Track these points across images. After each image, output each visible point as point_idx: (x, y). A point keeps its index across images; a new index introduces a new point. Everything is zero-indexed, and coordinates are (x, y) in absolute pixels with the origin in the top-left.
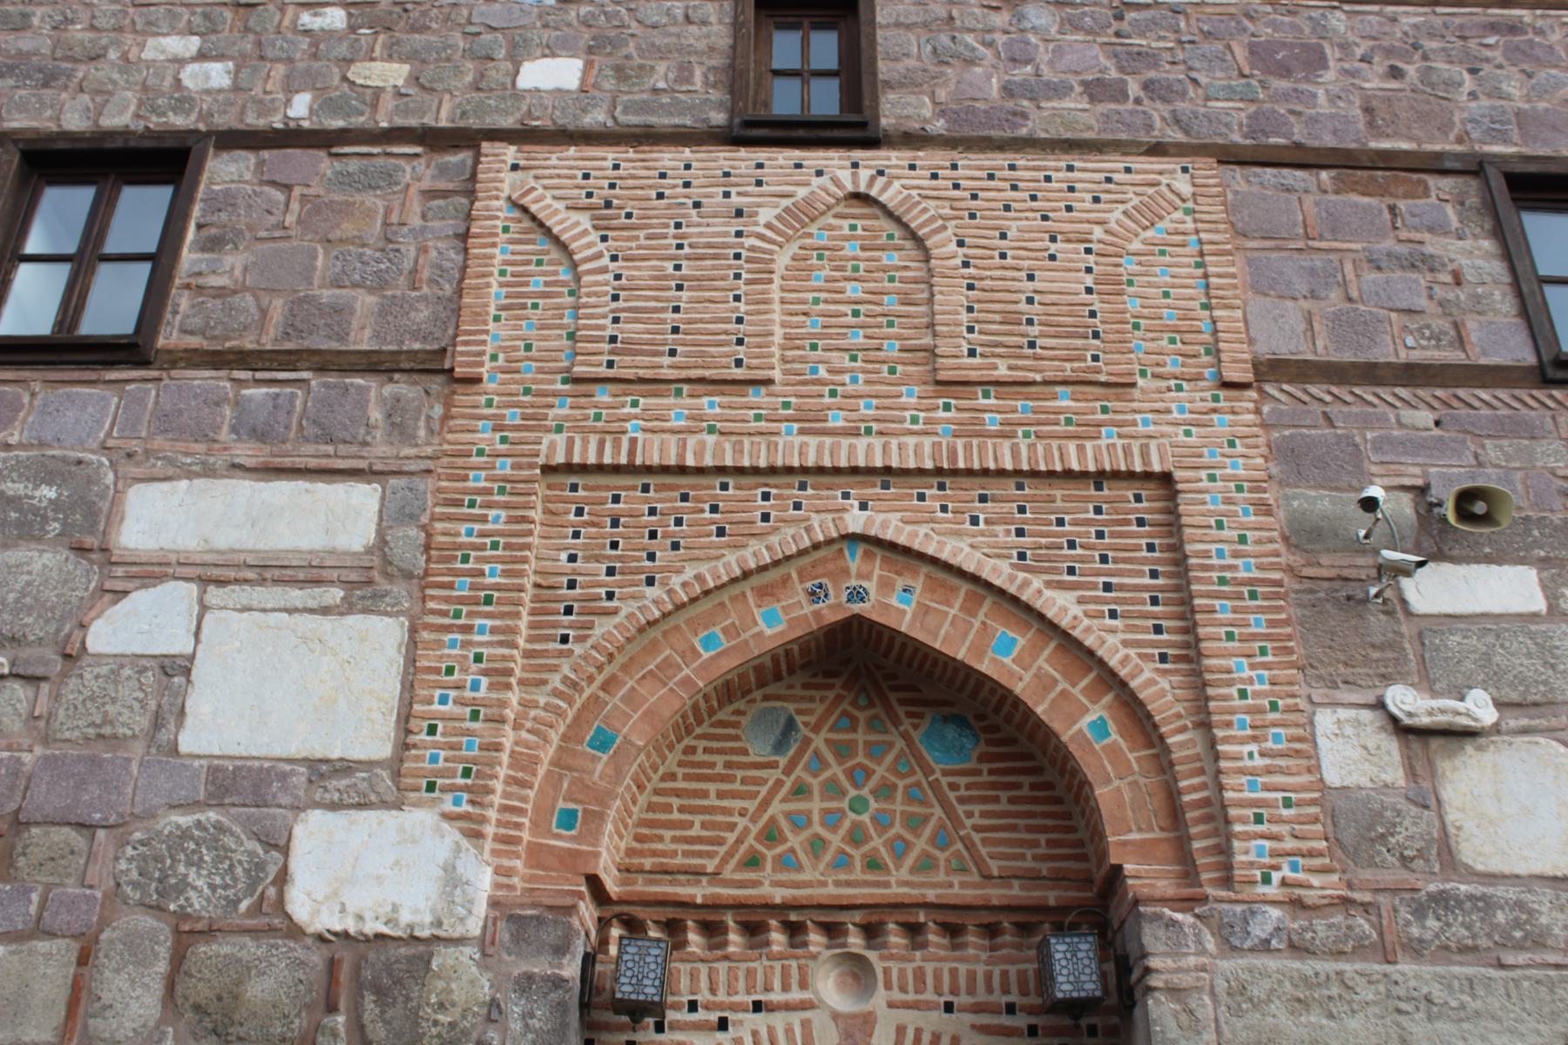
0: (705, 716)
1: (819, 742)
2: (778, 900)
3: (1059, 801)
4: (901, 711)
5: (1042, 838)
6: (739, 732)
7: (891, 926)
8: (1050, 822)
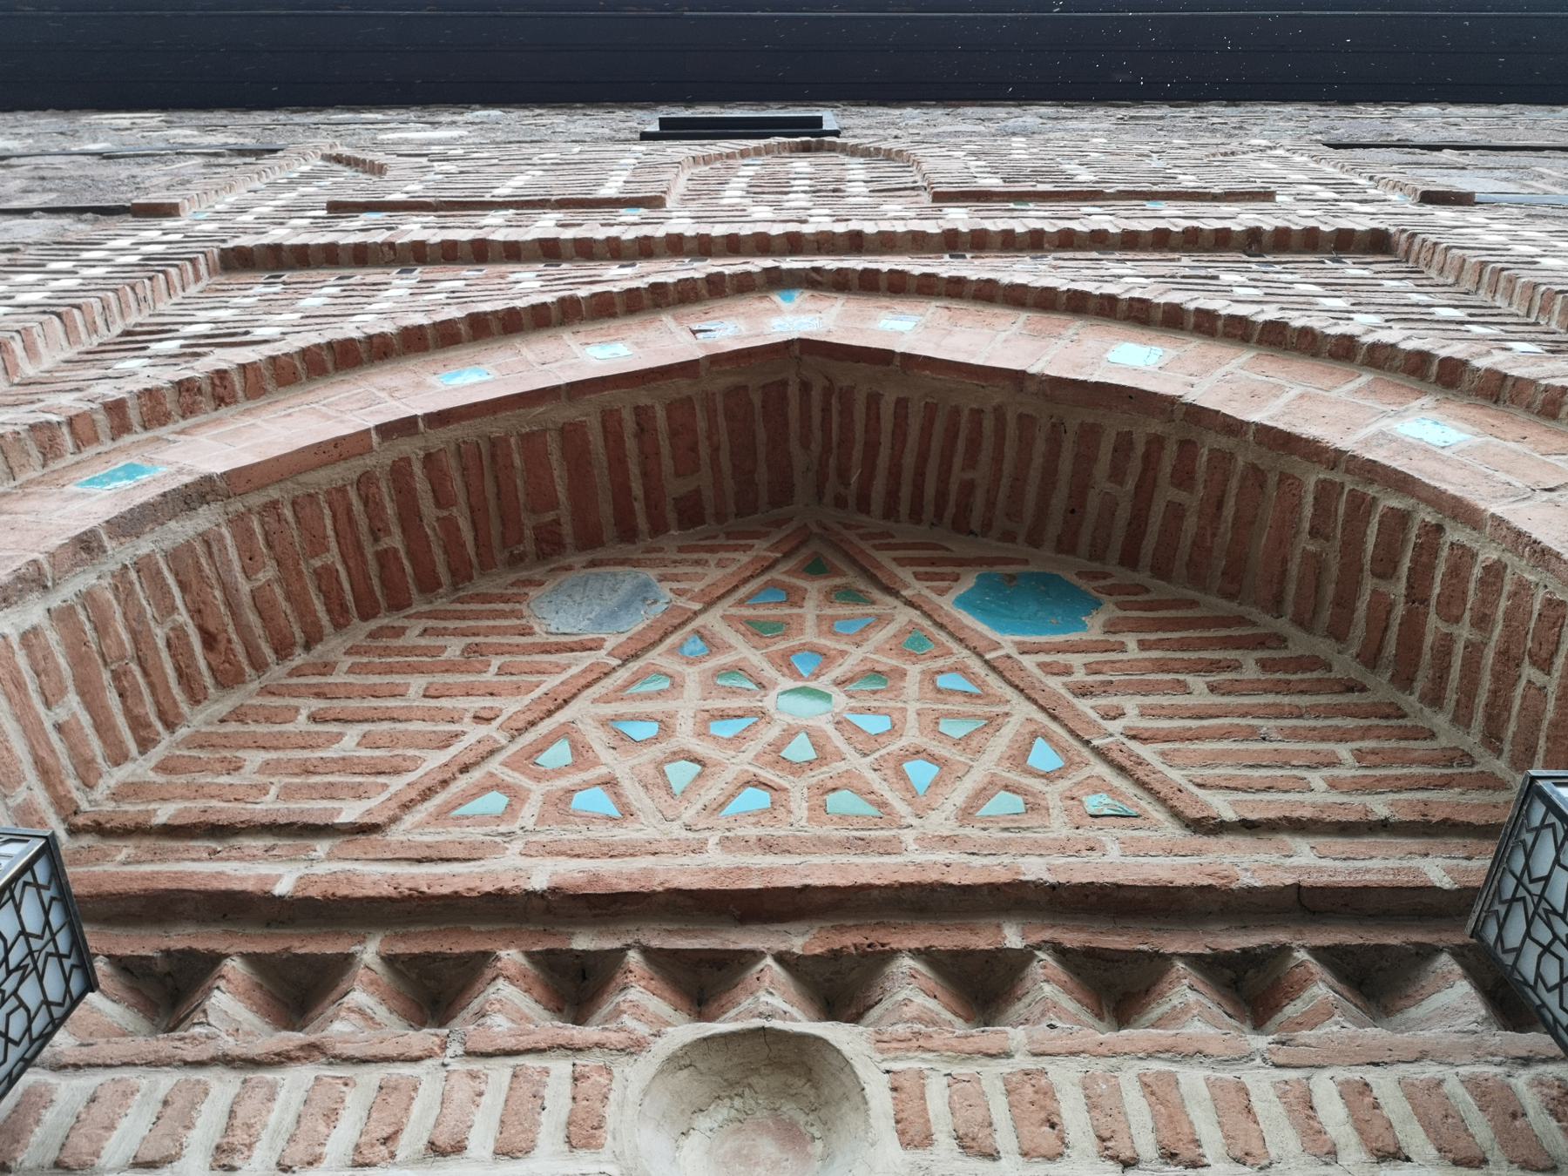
0: (444, 577)
1: (712, 620)
2: (539, 882)
3: (1350, 687)
4: (905, 574)
5: (1344, 751)
6: (523, 607)
7: (906, 963)
8: (1350, 723)
